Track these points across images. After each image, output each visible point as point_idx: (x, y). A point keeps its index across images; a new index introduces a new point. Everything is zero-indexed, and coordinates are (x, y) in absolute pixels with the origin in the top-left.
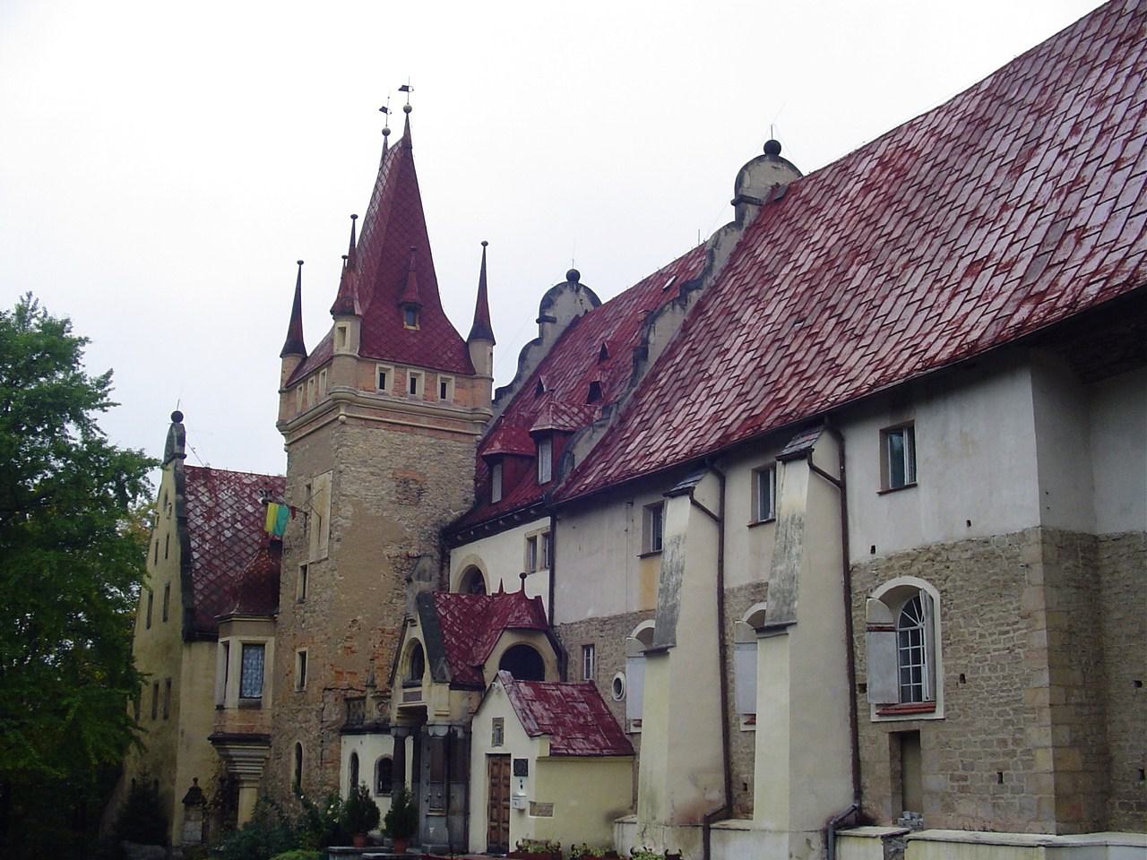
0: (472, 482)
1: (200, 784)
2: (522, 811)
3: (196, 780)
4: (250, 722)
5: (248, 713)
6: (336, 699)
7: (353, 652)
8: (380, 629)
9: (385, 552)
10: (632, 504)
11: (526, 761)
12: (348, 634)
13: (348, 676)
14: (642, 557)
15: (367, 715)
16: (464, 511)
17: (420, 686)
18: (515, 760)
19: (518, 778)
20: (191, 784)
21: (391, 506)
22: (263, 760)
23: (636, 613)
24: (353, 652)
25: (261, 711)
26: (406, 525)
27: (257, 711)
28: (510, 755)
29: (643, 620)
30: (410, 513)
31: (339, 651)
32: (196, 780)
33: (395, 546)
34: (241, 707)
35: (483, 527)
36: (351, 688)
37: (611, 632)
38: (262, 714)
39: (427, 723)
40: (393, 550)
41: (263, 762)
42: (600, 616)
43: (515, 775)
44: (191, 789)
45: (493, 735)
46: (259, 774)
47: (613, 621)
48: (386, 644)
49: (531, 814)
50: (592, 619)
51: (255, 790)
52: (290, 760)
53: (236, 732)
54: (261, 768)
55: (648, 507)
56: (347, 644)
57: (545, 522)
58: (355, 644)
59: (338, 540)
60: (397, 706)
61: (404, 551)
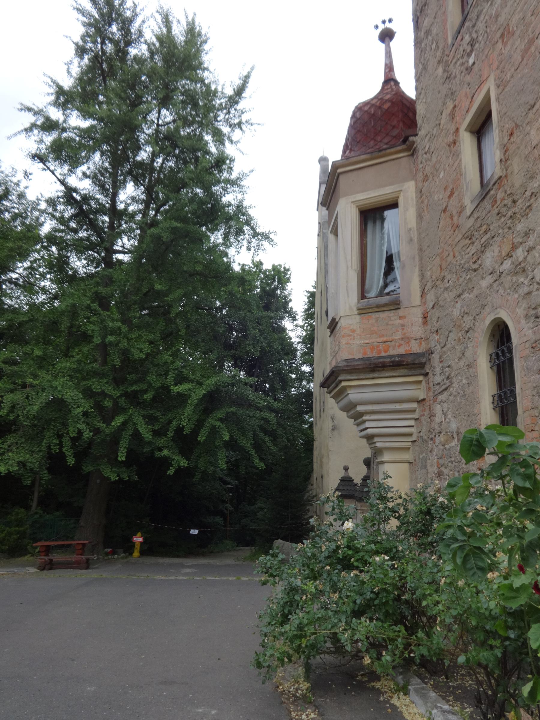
1: (351, 473)
3: (346, 469)
4: (382, 336)
5: (377, 319)
20: (342, 474)
22: (414, 405)
25: (401, 312)
27: (391, 314)
32: (346, 469)
34: (362, 311)
38: (401, 318)
41: (413, 411)
44: (342, 480)
46: (410, 435)
51: (406, 465)
52: (472, 380)
53: (358, 355)
54: (412, 423)
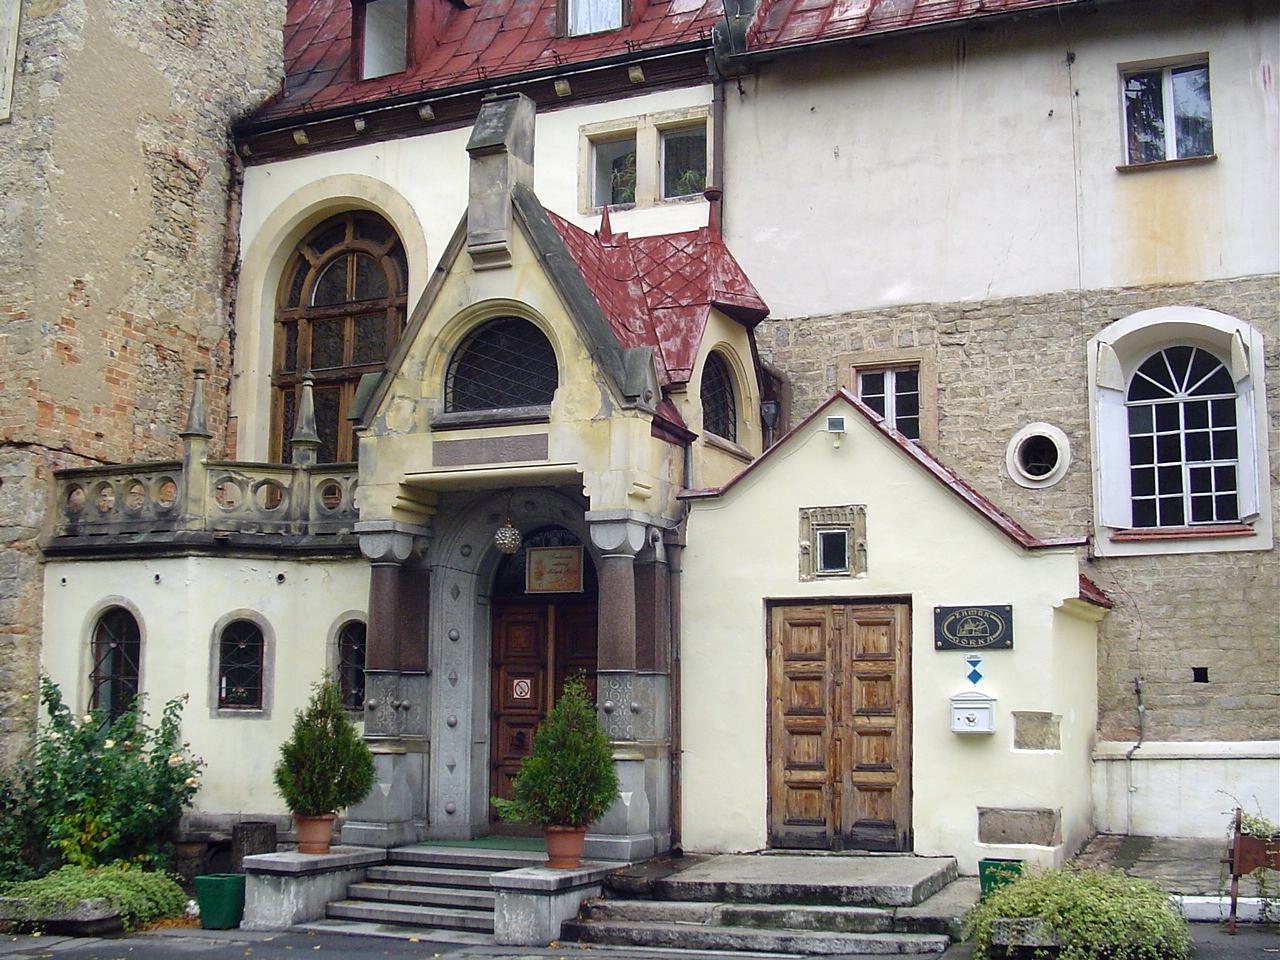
0: (280, 36)
2: (975, 740)
6: (38, 472)
7: (73, 359)
8: (124, 315)
9: (140, 137)
10: (1071, 58)
11: (1005, 613)
12: (66, 313)
13: (62, 416)
14: (1122, 171)
15: (193, 508)
16: (268, 94)
17: (545, 420)
18: (941, 614)
19: (958, 660)
21: (155, 34)
23: (1110, 292)
24: (73, 359)
26: (176, 88)
28: (906, 600)
29: (1142, 307)
30: (183, 61)
31: (48, 352)
33: (157, 130)
35: (415, 110)
36: (68, 449)
37: (1000, 334)
39: (589, 516)
40: (151, 136)
42: (942, 298)
43: (943, 644)
45: (805, 551)
47: (1003, 311)
48: (132, 354)
49: (1019, 744)
50: (903, 308)
55: (1127, 75)
56: (65, 338)
57: (689, 101)
58: (76, 339)
59: (57, 77)
60: (399, 476)
61: (171, 145)
